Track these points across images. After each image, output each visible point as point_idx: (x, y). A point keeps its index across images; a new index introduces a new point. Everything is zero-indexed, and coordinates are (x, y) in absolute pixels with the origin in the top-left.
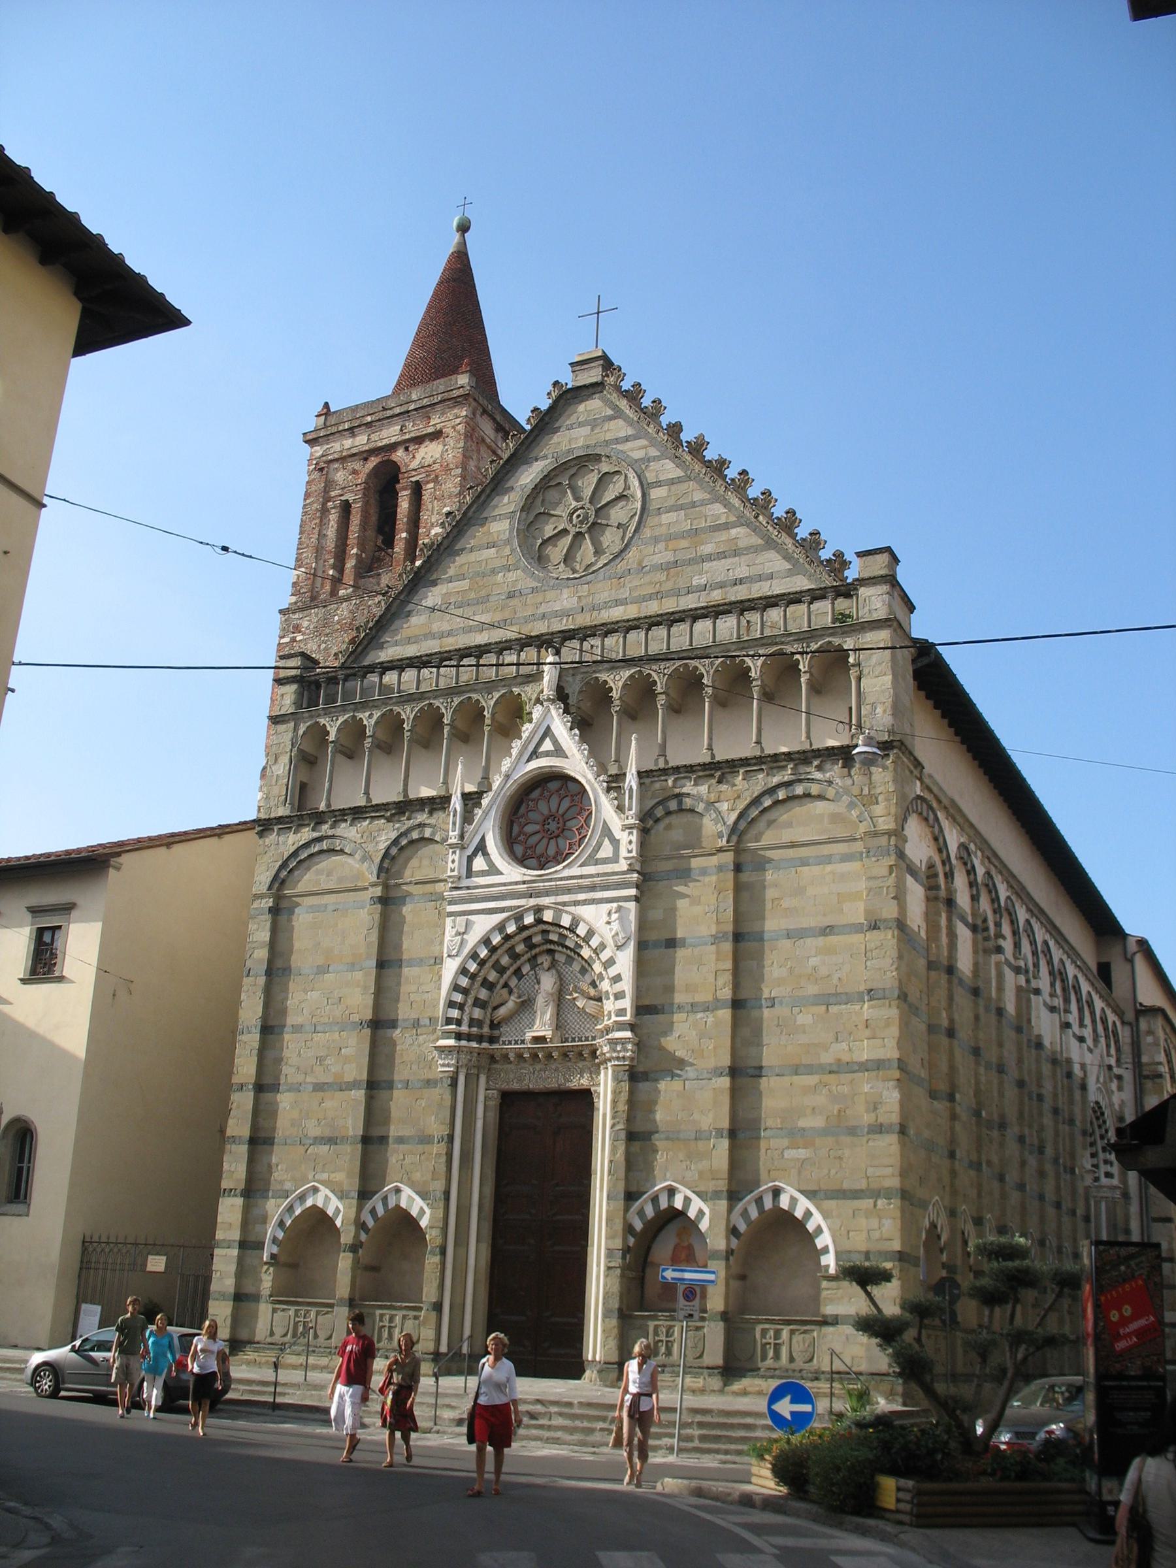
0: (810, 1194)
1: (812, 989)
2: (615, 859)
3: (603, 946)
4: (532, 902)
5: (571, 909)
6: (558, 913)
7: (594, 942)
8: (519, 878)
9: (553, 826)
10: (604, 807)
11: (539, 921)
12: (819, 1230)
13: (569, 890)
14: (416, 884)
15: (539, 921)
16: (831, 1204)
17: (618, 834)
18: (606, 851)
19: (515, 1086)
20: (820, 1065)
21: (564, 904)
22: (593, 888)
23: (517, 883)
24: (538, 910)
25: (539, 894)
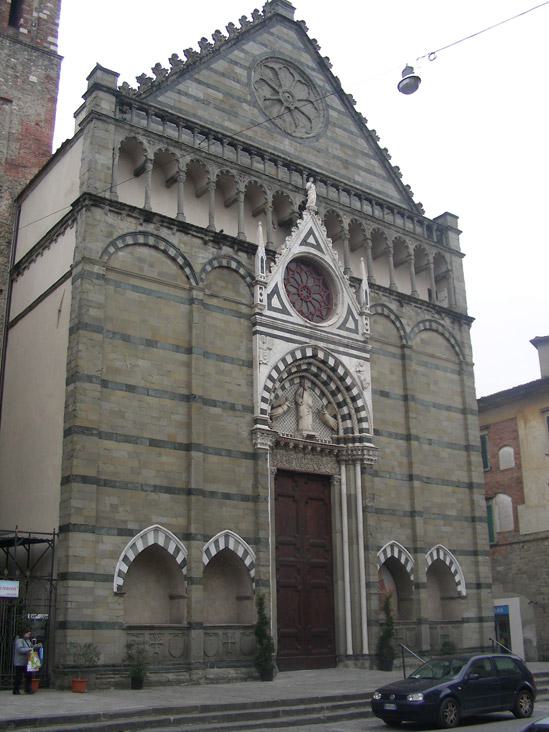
0: (454, 552)
1: (446, 439)
2: (356, 331)
3: (354, 384)
4: (313, 342)
5: (336, 355)
6: (327, 355)
7: (348, 381)
8: (302, 323)
9: (305, 293)
10: (345, 298)
11: (314, 356)
12: (456, 572)
13: (333, 343)
14: (225, 300)
15: (314, 356)
16: (460, 557)
17: (357, 317)
18: (351, 324)
19: (286, 466)
20: (452, 482)
21: (332, 350)
22: (347, 346)
23: (300, 325)
24: (315, 348)
25: (316, 339)
